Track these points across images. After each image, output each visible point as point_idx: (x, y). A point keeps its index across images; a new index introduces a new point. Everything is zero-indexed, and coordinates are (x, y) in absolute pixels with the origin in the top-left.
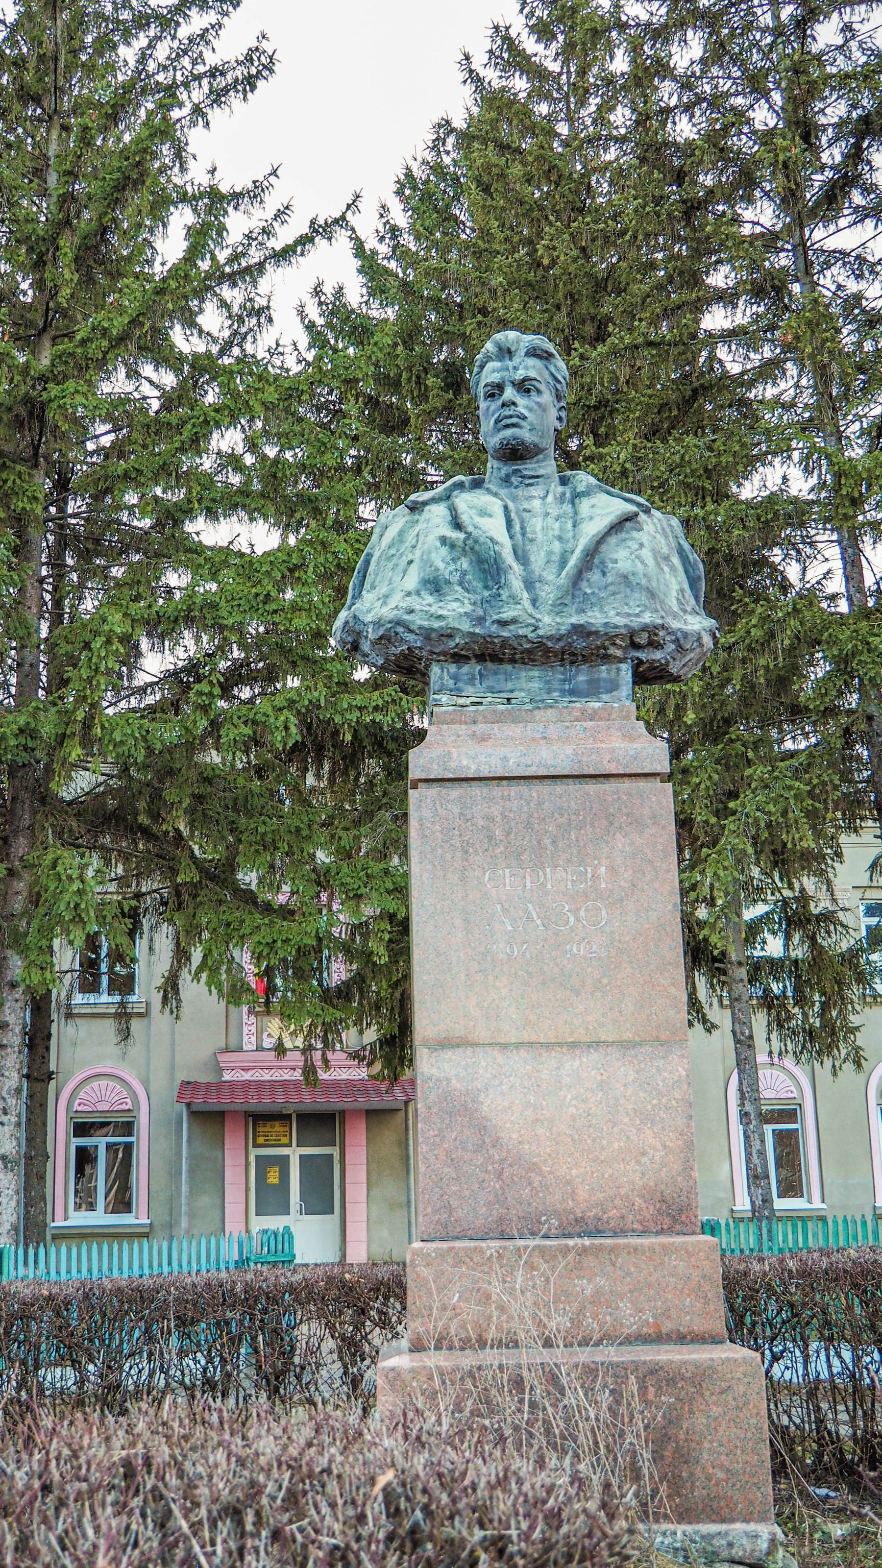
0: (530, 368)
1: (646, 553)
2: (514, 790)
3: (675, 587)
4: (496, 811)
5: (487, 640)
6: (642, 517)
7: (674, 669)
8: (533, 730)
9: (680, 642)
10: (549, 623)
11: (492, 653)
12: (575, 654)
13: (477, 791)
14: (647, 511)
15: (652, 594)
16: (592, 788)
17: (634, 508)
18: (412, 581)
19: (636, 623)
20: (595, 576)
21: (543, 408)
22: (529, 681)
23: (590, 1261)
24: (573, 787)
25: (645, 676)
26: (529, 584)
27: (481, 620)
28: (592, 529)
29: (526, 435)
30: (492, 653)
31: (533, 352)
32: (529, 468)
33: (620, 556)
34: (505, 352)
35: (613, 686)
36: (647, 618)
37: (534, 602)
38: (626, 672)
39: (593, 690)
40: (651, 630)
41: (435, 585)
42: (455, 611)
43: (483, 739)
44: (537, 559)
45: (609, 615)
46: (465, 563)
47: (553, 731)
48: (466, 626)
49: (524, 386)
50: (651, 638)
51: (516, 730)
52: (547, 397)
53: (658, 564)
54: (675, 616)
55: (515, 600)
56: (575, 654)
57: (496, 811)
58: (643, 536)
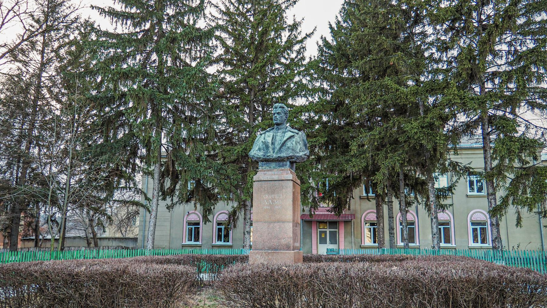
0: (279, 110)
1: (294, 143)
2: (269, 182)
3: (299, 147)
4: (266, 186)
5: (265, 159)
6: (296, 135)
7: (298, 161)
8: (273, 173)
9: (298, 158)
10: (275, 156)
11: (267, 161)
12: (279, 161)
13: (263, 183)
14: (298, 134)
15: (293, 150)
16: (280, 182)
17: (292, 134)
18: (257, 149)
19: (288, 155)
20: (284, 147)
21: (282, 117)
22: (273, 165)
23: (275, 254)
24: (277, 182)
25: (292, 163)
26: (274, 149)
27: (264, 156)
28: (285, 139)
29: (278, 122)
30: (267, 161)
31: (280, 107)
32: (279, 127)
33: (289, 144)
34: (276, 108)
35: (286, 165)
36: (291, 154)
37: (274, 152)
38: (288, 163)
39: (283, 166)
40: (291, 156)
41: (259, 149)
42: (261, 154)
43: (265, 174)
44: (276, 144)
45: (283, 155)
46: (264, 146)
47: (276, 173)
48: (262, 157)
49: (278, 113)
50: (291, 157)
51: (270, 173)
52: (283, 114)
53: (296, 144)
54: (298, 153)
55: (270, 152)
56: (279, 161)
57: (266, 186)
58: (294, 139)
